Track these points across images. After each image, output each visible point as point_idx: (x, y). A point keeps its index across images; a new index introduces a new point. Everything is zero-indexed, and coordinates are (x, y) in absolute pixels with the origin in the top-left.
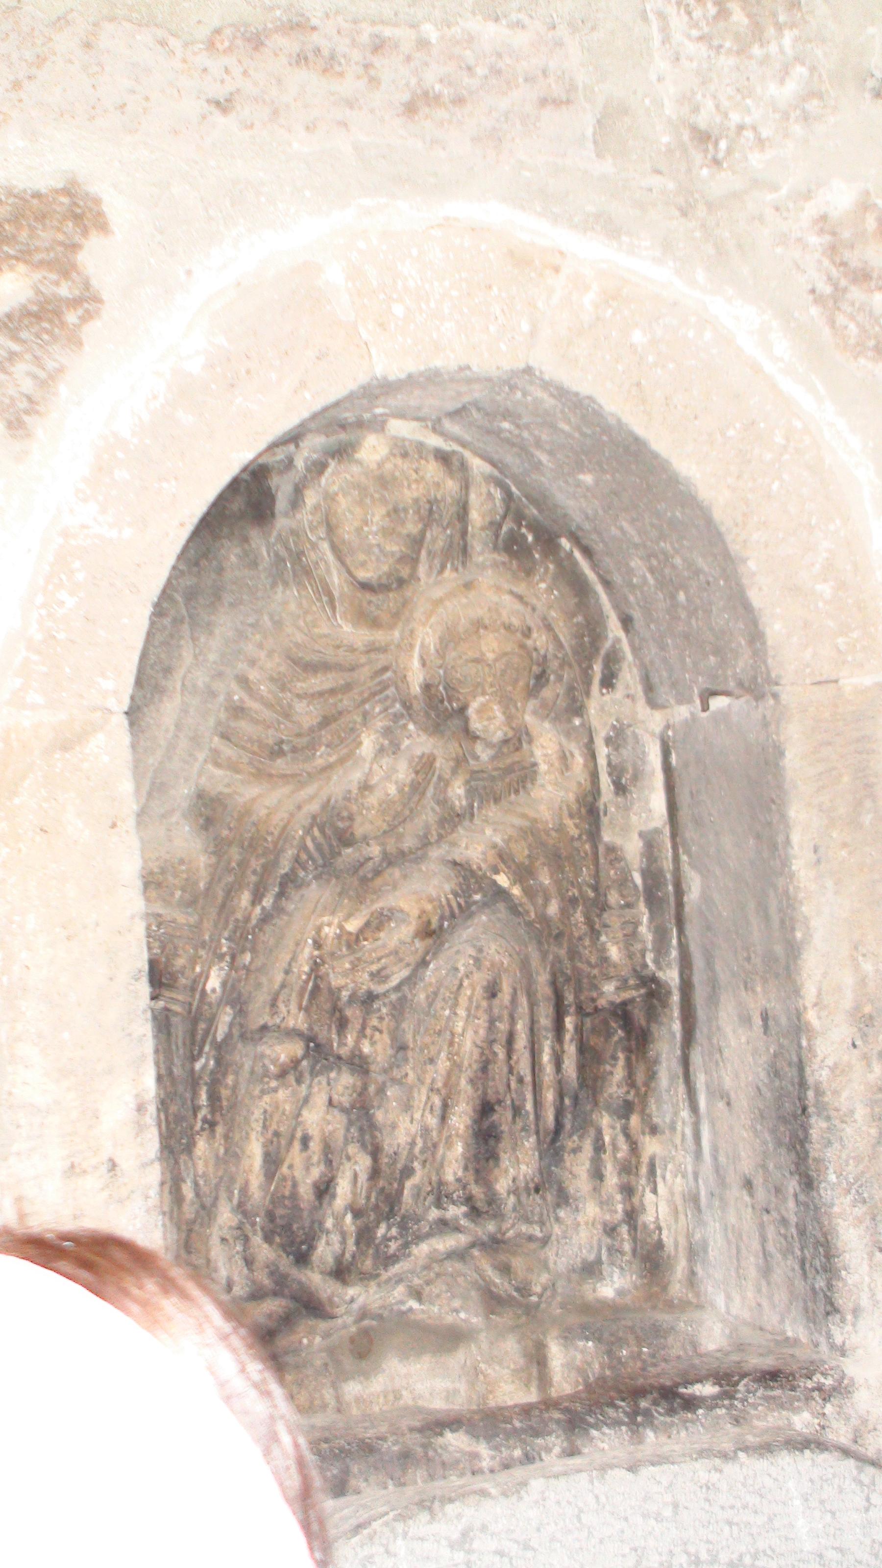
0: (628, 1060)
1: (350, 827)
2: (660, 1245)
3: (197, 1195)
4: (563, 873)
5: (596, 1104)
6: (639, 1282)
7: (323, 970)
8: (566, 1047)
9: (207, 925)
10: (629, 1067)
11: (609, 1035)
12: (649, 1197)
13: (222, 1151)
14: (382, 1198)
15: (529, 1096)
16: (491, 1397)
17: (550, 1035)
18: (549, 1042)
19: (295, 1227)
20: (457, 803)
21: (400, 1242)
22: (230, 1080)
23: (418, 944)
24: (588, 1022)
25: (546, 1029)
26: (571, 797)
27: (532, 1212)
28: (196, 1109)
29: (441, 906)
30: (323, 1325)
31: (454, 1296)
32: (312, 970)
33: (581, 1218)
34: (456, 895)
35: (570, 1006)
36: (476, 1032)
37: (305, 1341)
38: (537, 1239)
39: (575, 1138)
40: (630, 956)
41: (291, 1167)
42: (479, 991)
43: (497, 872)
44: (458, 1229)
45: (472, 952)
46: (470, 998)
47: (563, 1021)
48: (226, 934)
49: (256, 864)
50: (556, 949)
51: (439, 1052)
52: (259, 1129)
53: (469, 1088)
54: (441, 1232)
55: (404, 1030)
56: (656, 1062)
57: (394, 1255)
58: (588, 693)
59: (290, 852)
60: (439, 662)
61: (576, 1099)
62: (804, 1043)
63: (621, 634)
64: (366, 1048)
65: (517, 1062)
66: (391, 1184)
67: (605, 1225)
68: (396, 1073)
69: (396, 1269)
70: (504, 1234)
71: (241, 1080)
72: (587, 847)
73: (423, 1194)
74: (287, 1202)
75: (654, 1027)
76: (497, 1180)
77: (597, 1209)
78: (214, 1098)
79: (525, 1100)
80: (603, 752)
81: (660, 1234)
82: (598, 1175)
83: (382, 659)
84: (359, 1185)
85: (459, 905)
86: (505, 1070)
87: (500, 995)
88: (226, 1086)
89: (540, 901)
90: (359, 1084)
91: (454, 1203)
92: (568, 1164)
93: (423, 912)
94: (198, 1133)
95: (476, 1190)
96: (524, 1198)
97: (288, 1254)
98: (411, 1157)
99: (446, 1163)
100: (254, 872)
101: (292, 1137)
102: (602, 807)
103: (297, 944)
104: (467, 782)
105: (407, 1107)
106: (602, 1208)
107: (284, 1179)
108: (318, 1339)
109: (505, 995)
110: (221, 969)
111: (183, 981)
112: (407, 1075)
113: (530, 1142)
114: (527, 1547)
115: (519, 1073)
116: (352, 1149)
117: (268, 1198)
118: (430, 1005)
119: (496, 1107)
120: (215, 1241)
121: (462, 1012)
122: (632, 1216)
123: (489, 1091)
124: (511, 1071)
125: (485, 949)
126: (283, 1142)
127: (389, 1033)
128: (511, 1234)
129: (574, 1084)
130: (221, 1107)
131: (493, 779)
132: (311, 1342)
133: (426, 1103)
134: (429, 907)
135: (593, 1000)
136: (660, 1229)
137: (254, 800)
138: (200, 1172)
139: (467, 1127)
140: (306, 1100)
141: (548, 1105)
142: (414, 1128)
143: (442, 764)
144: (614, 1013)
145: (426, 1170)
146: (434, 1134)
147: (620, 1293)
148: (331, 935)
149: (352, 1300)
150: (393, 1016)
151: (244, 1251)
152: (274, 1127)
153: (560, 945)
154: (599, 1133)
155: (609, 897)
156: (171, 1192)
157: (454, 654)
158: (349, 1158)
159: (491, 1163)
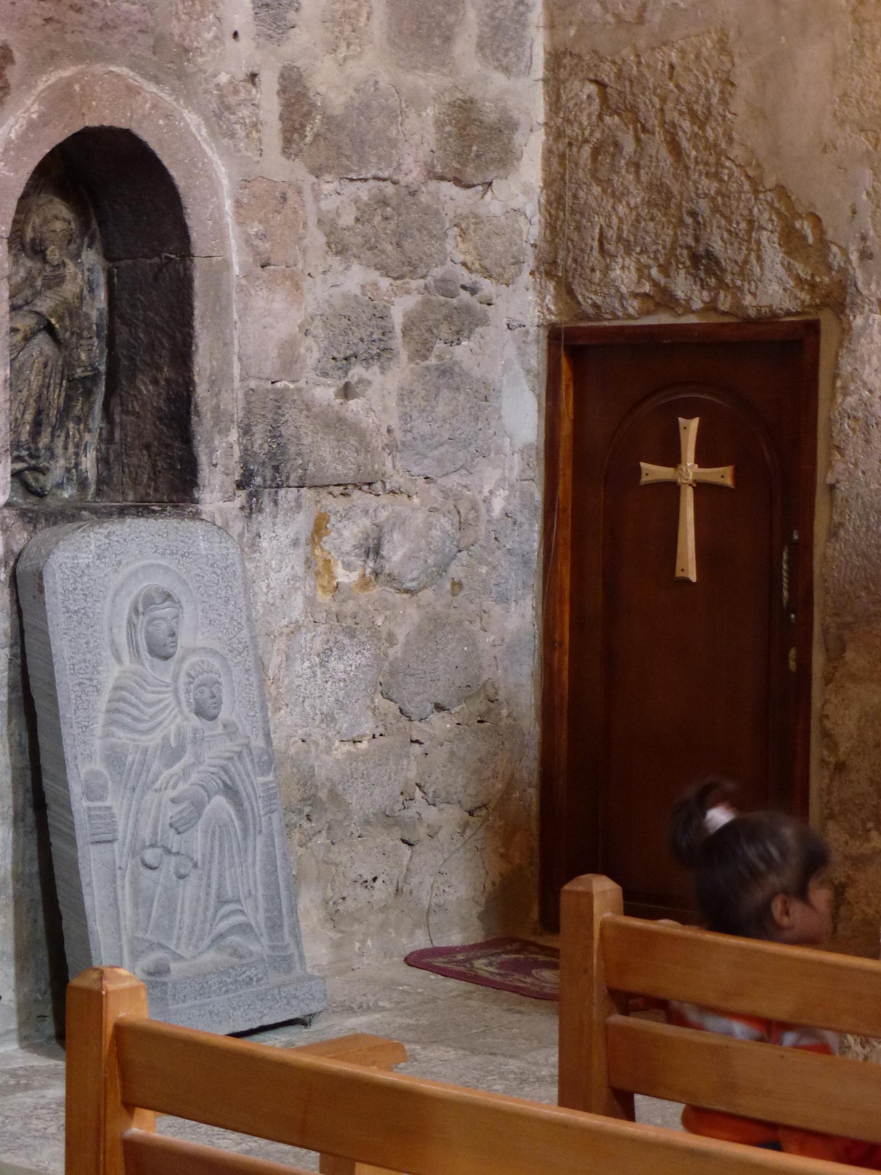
2: (86, 478)
10: (83, 404)
12: (84, 459)
33: (58, 465)
40: (90, 358)
42: (41, 366)
43: (52, 317)
56: (94, 403)
67: (66, 468)
75: (94, 389)
82: (66, 448)
95: (32, 446)
109: (49, 369)
114: (125, 540)
121: (34, 372)
122: (77, 465)
131: (50, 279)
147: (71, 496)
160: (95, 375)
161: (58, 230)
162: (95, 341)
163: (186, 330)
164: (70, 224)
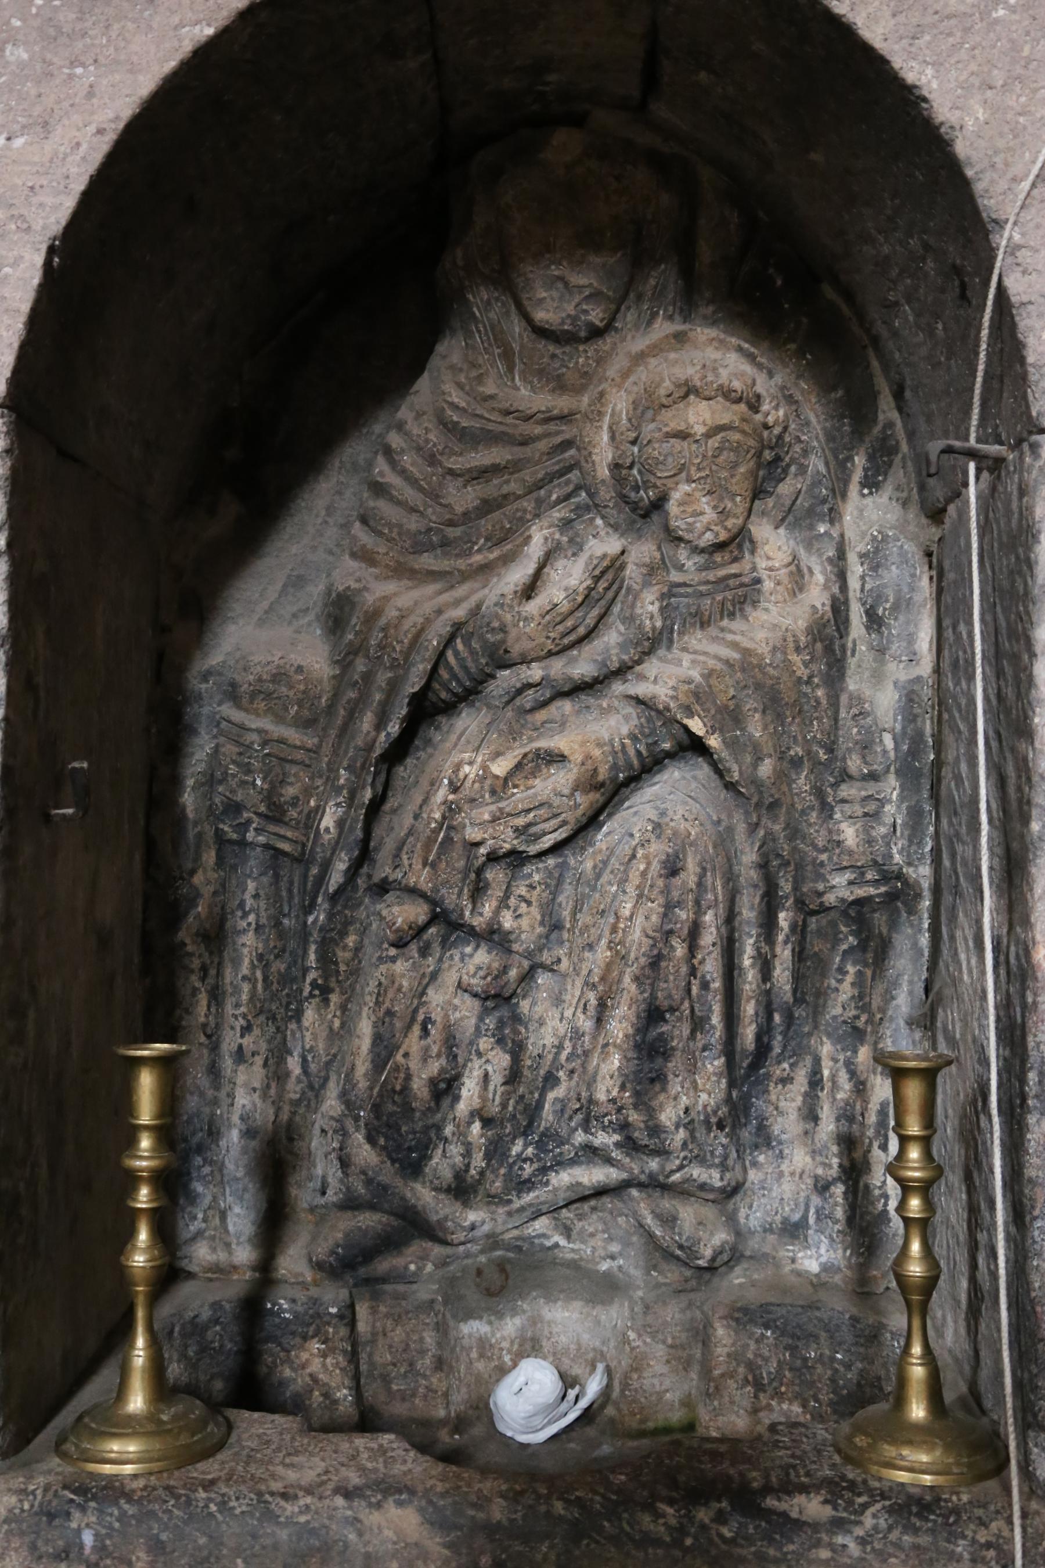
0: (860, 974)
1: (503, 641)
3: (305, 1071)
4: (782, 725)
5: (816, 1027)
7: (459, 819)
8: (778, 950)
9: (327, 749)
10: (859, 982)
11: (836, 941)
13: (337, 1023)
14: (520, 1107)
16: (635, 1376)
18: (751, 941)
19: (404, 1129)
21: (536, 1166)
22: (351, 940)
23: (579, 797)
24: (813, 923)
25: (748, 923)
26: (802, 624)
27: (712, 1153)
28: (305, 970)
30: (438, 1250)
31: (611, 1239)
32: (444, 817)
34: (634, 738)
35: (787, 898)
37: (412, 1267)
38: (712, 1189)
39: (786, 1065)
40: (870, 842)
41: (406, 1055)
42: (656, 866)
43: (691, 714)
44: (609, 1161)
46: (644, 874)
47: (777, 917)
48: (345, 764)
49: (383, 677)
50: (770, 825)
52: (371, 1004)
53: (633, 987)
54: (589, 1162)
55: (560, 905)
56: (896, 984)
57: (528, 1180)
58: (844, 495)
59: (421, 667)
61: (789, 1019)
62: (1030, 1000)
63: (895, 416)
64: (507, 922)
65: (702, 962)
66: (532, 1093)
67: (816, 1178)
68: (546, 957)
69: (529, 1198)
70: (668, 1177)
71: (366, 941)
74: (396, 1098)
76: (661, 1105)
77: (808, 1159)
78: (326, 960)
79: (710, 1010)
80: (856, 570)
81: (886, 1204)
82: (811, 1115)
83: (567, 432)
84: (491, 1088)
85: (639, 753)
86: (684, 970)
87: (683, 875)
88: (345, 948)
89: (748, 759)
90: (496, 965)
91: (604, 1129)
92: (773, 1097)
93: (588, 757)
94: (307, 999)
95: (634, 1117)
96: (700, 1133)
97: (393, 1161)
98: (556, 1065)
99: (599, 1078)
101: (413, 1020)
102: (850, 645)
103: (432, 784)
104: (662, 597)
105: (558, 1001)
106: (813, 1159)
107: (397, 1068)
108: (429, 1267)
109: (689, 876)
110: (338, 805)
111: (293, 813)
112: (559, 961)
113: (715, 1064)
115: (703, 976)
116: (484, 1043)
118: (598, 876)
120: (317, 1131)
121: (631, 889)
123: (659, 994)
124: (693, 972)
125: (670, 813)
126: (398, 1024)
127: (541, 906)
128: (676, 1177)
129: (788, 997)
130: (338, 972)
131: (702, 595)
132: (420, 1269)
134: (597, 753)
135: (820, 894)
137: (386, 599)
138: (308, 1047)
139: (626, 1036)
140: (434, 976)
141: (747, 1020)
143: (632, 572)
144: (845, 913)
145: (573, 1083)
146: (587, 1038)
147: (826, 1268)
149: (473, 1227)
150: (547, 886)
151: (341, 1149)
152: (387, 1004)
153: (775, 819)
154: (817, 1061)
155: (849, 763)
156: (265, 1065)
157: (652, 426)
158: (479, 1055)
159: (657, 1087)
160: (892, 897)
161: (699, 430)
162: (891, 787)
163: (1022, 746)
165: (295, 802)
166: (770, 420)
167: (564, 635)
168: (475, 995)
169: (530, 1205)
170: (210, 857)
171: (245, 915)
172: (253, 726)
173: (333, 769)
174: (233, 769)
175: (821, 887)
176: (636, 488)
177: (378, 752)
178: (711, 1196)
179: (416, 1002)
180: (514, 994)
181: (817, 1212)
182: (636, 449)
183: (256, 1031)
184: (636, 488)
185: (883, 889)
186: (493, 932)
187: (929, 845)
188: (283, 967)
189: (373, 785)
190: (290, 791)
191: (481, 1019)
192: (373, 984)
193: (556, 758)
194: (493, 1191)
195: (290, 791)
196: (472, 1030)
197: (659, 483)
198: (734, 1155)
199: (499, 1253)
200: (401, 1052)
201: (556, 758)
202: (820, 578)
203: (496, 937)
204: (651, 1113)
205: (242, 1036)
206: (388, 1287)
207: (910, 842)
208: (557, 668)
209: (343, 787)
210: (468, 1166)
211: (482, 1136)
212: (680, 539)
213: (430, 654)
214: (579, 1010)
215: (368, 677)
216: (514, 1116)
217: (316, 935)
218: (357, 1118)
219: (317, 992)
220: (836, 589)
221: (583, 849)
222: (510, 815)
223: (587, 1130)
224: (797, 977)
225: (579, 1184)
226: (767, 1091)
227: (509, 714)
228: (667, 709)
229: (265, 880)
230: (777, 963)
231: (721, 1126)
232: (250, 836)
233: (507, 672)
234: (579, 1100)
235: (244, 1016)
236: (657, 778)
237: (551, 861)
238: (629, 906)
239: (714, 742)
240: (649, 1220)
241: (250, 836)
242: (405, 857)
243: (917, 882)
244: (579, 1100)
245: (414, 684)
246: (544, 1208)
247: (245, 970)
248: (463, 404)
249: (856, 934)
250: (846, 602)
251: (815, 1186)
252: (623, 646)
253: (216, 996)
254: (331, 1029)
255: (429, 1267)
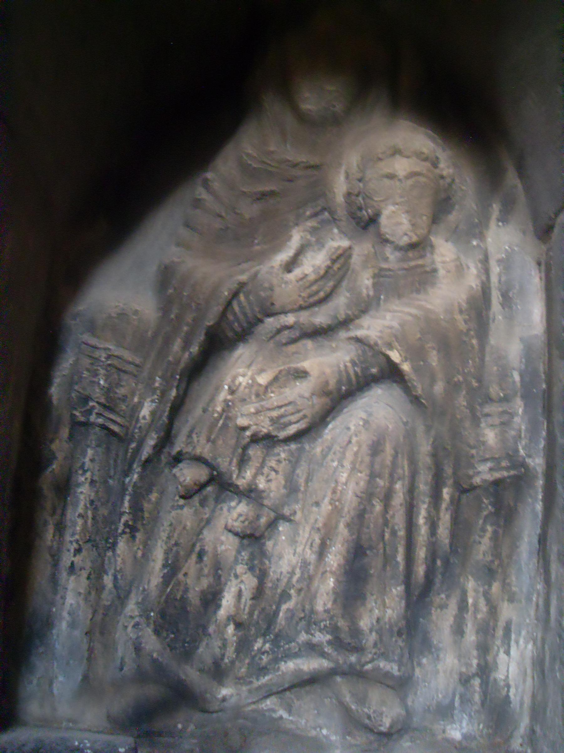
0: (495, 532)
1: (271, 297)
3: (116, 587)
6: (485, 731)
8: (442, 514)
9: (148, 365)
10: (495, 538)
11: (480, 509)
12: (502, 656)
13: (140, 553)
15: (401, 550)
17: (427, 500)
18: (425, 506)
20: (365, 291)
21: (271, 656)
22: (154, 496)
23: (315, 400)
24: (464, 497)
26: (464, 297)
29: (340, 372)
30: (198, 716)
32: (223, 410)
33: (440, 667)
34: (354, 363)
36: (357, 483)
37: (180, 726)
38: (392, 677)
39: (443, 596)
41: (186, 574)
42: (365, 449)
44: (323, 655)
45: (363, 415)
46: (356, 454)
47: (441, 492)
48: (160, 373)
49: (189, 318)
51: (325, 496)
52: (165, 538)
55: (298, 476)
57: (265, 668)
60: (359, 175)
61: (447, 563)
64: (262, 484)
65: (393, 516)
66: (271, 606)
67: (461, 674)
68: (286, 511)
69: (265, 680)
70: (363, 665)
72: (474, 341)
73: (296, 619)
77: (456, 661)
79: (396, 550)
80: (495, 270)
81: (508, 691)
84: (243, 600)
85: (356, 374)
86: (381, 521)
88: (149, 501)
90: (251, 514)
91: (320, 631)
92: (434, 617)
94: (121, 534)
95: (341, 623)
97: (172, 649)
98: (289, 584)
99: (318, 595)
100: (188, 324)
104: (375, 276)
105: (293, 541)
106: (459, 661)
107: (179, 583)
108: (192, 727)
110: (153, 401)
112: (295, 513)
113: (398, 590)
116: (240, 569)
117: (164, 597)
119: (368, 552)
121: (347, 464)
123: (364, 537)
126: (182, 553)
128: (369, 667)
130: (143, 518)
132: (185, 728)
133: (308, 539)
134: (328, 371)
135: (471, 477)
136: (508, 686)
138: (118, 568)
139: (339, 565)
140: (208, 522)
141: (420, 562)
142: (294, 560)
143: (356, 259)
145: (300, 598)
146: (311, 567)
147: (465, 737)
148: (244, 384)
149: (224, 699)
150: (290, 461)
155: (491, 390)
156: (88, 578)
158: (236, 576)
161: (401, 173)
162: (519, 406)
164: (435, 164)
165: (124, 398)
166: (445, 173)
167: (310, 296)
168: (236, 534)
169: (265, 685)
170: (65, 432)
171: (85, 472)
172: (102, 346)
173: (151, 379)
174: (86, 374)
175: (471, 472)
176: (360, 209)
177: (182, 365)
178: (391, 683)
179: (195, 538)
180: (262, 536)
181: (461, 697)
182: (361, 185)
183: (84, 553)
184: (360, 209)
185: (512, 472)
186: (251, 491)
187: (542, 444)
188: (106, 513)
189: (177, 388)
190: (121, 391)
191: (239, 552)
192: (166, 524)
193: (302, 374)
194: (240, 675)
195: (121, 391)
196: (232, 559)
197: (375, 204)
198: (407, 655)
199: (241, 721)
200: (183, 572)
201: (302, 374)
202: (474, 271)
203: (253, 495)
204: (353, 620)
205: (75, 555)
206: (163, 740)
207: (530, 440)
208: (304, 317)
209: (156, 389)
210: (223, 655)
211: (234, 635)
212: (387, 241)
213: (222, 301)
214: (308, 547)
215: (179, 317)
216: (258, 623)
217: (130, 489)
218: (148, 618)
219: (128, 530)
220: (484, 278)
221: (315, 439)
222: (269, 409)
223: (308, 632)
224: (453, 535)
225: (301, 670)
226: (430, 614)
227: (271, 344)
228: (376, 344)
229: (100, 450)
230: (440, 523)
231: (400, 634)
232: (93, 418)
233: (270, 320)
234: (303, 611)
235: (77, 541)
236: (367, 394)
237: (293, 446)
238: (345, 475)
239: (406, 367)
240: (348, 699)
241: (93, 418)
242: (194, 436)
243: (534, 469)
244: (303, 611)
245: (209, 322)
246: (275, 689)
247: (80, 510)
248: (255, 155)
249: (494, 505)
250: (489, 288)
251: (460, 680)
252: (348, 306)
253: (60, 528)
254: (135, 557)
255: (192, 727)
